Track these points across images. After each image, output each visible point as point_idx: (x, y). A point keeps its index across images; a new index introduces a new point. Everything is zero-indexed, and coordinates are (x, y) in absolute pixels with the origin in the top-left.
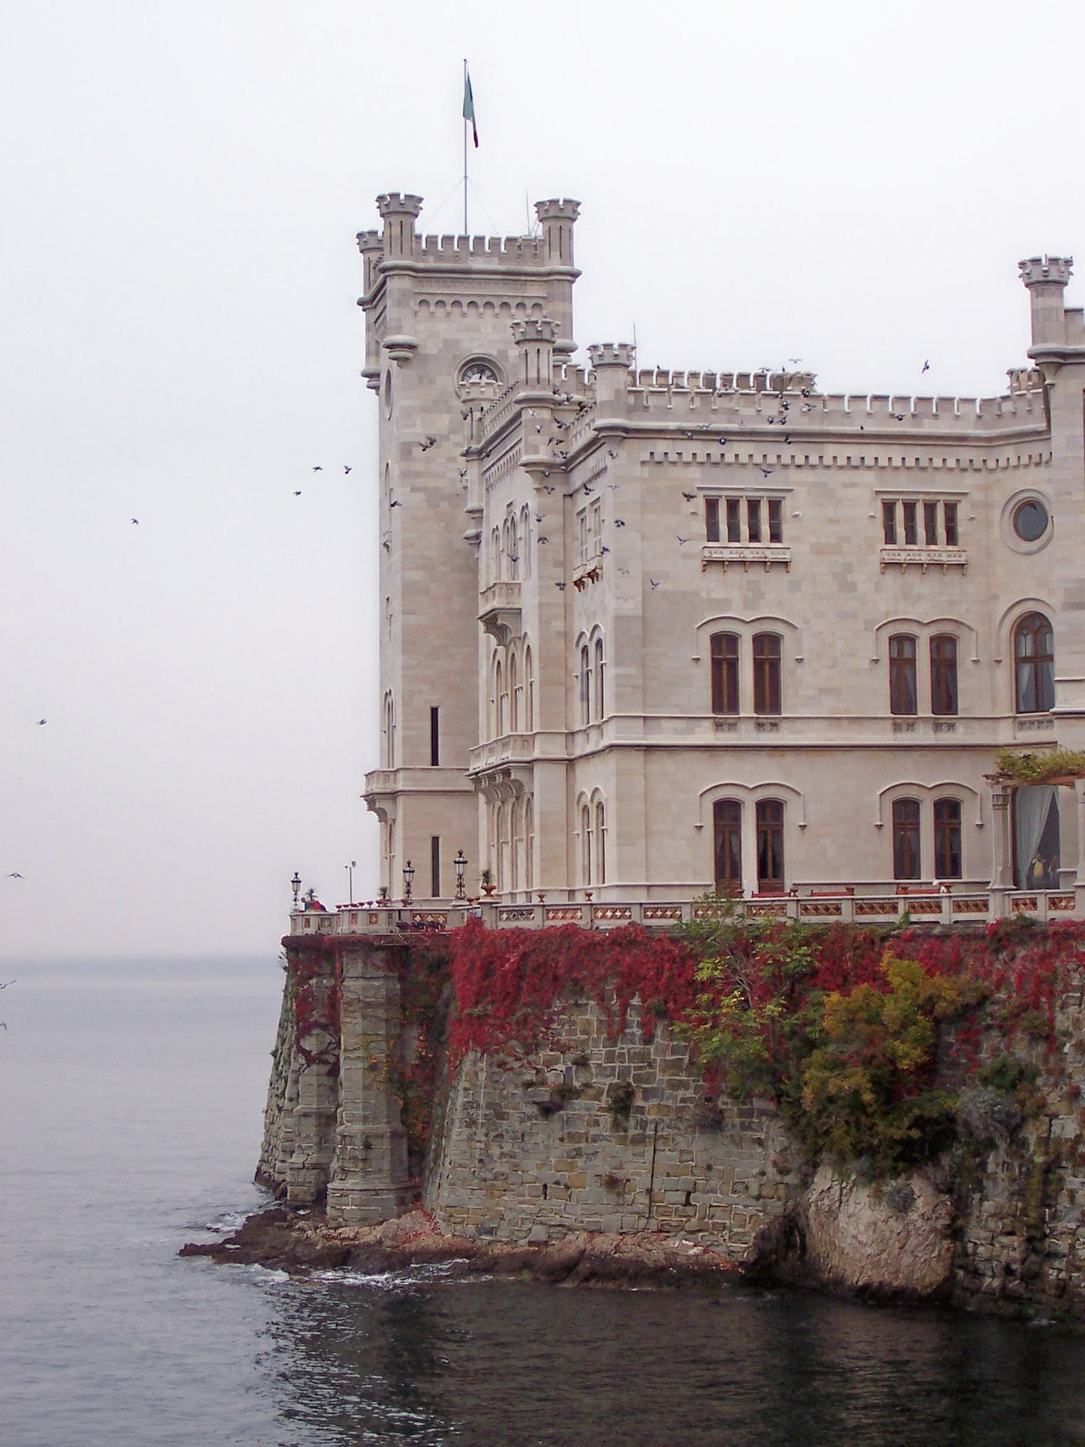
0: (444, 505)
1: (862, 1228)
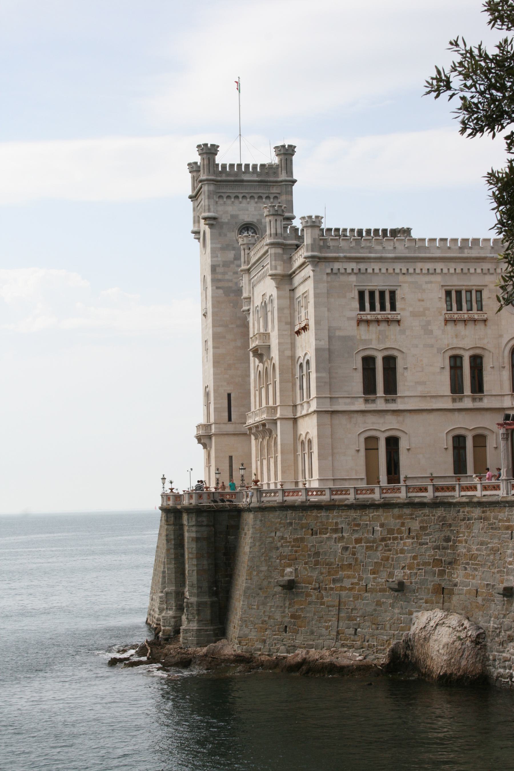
0: (232, 295)
1: (441, 647)
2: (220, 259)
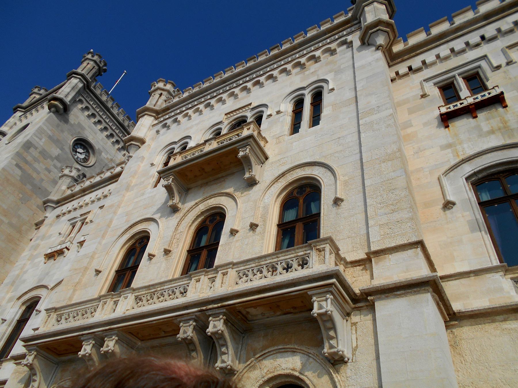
2: (42, 143)
